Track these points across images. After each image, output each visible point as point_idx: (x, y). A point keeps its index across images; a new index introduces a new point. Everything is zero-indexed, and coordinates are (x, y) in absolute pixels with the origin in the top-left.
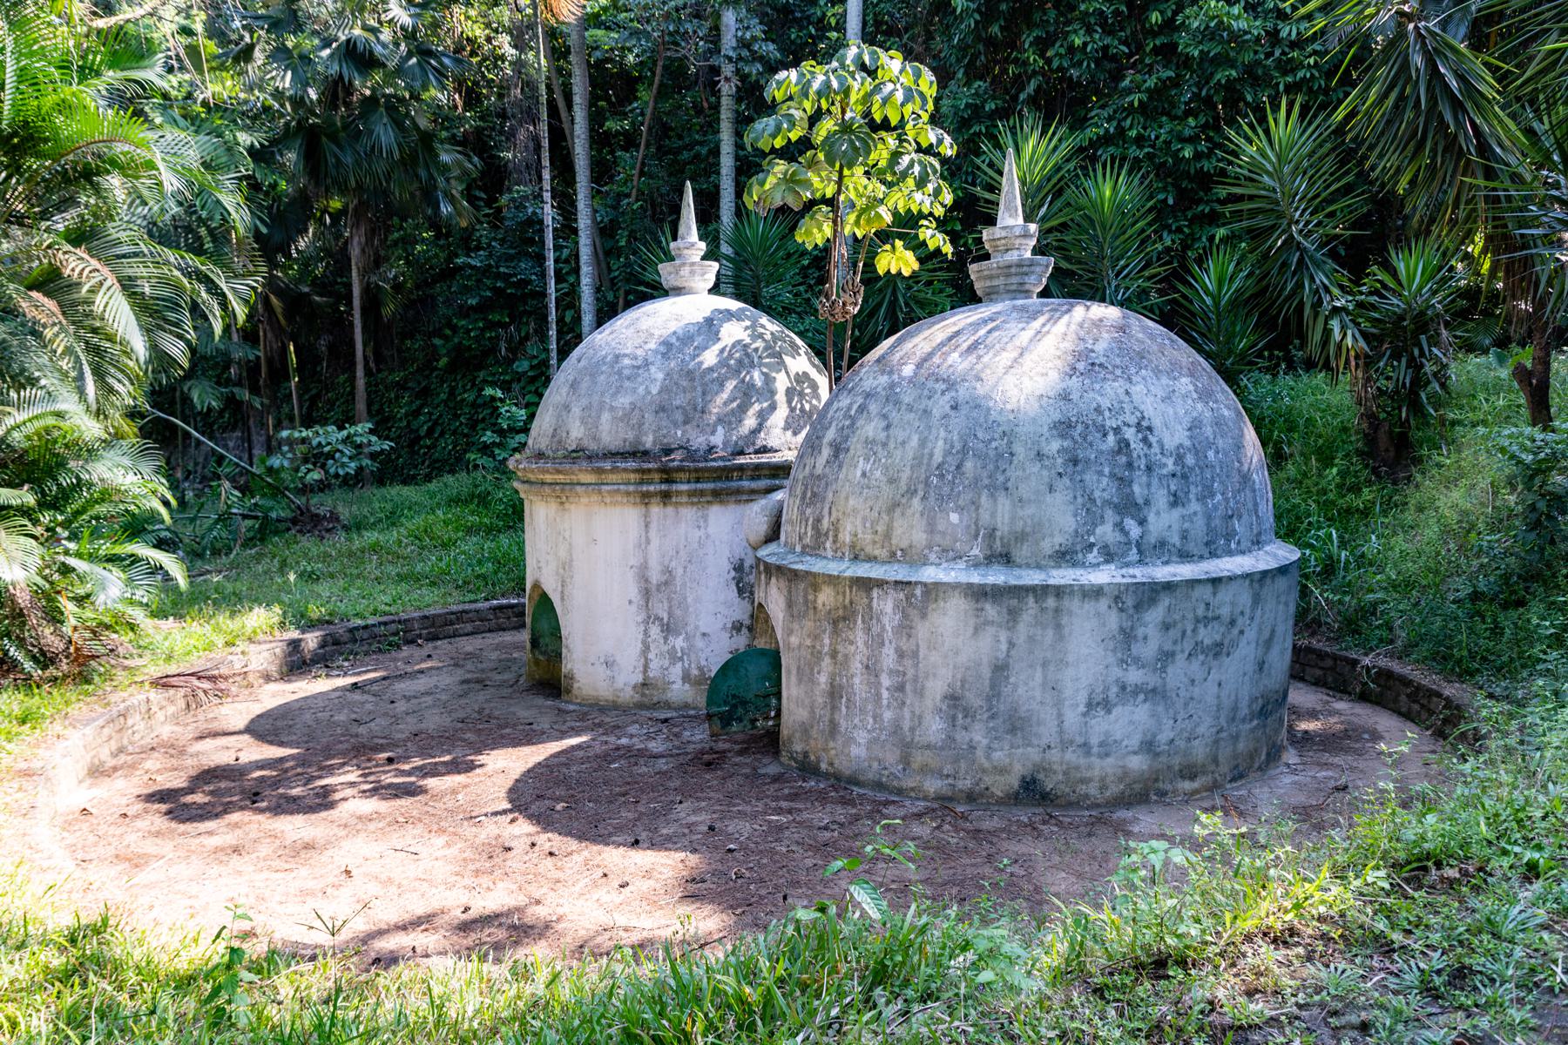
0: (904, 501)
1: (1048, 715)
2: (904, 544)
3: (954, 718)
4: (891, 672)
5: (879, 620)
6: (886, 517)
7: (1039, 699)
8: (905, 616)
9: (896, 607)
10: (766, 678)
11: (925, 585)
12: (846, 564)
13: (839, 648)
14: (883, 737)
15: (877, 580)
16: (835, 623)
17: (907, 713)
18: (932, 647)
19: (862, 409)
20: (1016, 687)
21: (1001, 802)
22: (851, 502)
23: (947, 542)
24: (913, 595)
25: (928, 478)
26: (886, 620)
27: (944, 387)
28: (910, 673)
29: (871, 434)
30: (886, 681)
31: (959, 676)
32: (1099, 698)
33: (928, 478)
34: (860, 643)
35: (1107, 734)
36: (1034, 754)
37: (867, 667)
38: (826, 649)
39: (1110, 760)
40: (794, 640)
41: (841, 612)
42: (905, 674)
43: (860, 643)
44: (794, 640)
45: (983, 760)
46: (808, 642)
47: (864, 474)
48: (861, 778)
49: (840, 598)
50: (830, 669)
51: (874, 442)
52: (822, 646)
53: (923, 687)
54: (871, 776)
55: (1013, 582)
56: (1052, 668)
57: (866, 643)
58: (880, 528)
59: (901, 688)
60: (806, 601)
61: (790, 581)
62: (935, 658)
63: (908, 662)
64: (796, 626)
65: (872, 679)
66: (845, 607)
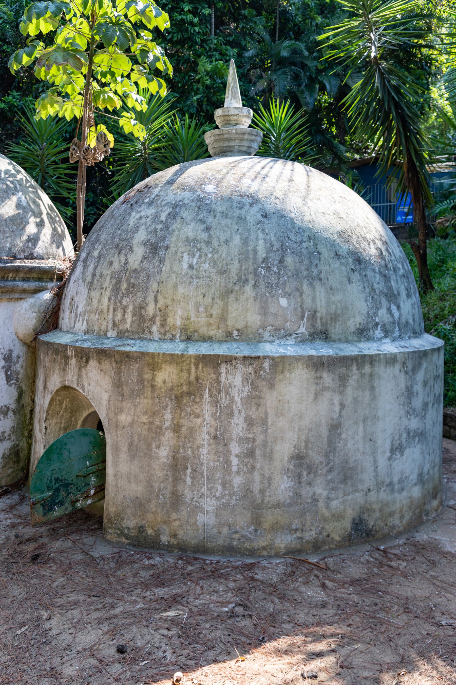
0: (237, 288)
1: (367, 462)
2: (240, 325)
3: (300, 476)
4: (241, 440)
5: (227, 393)
6: (220, 303)
7: (362, 450)
8: (254, 387)
9: (245, 379)
10: (87, 457)
11: (273, 359)
12: (182, 346)
13: (182, 421)
14: (233, 502)
15: (226, 357)
16: (178, 398)
17: (257, 477)
18: (279, 413)
19: (173, 216)
20: (346, 441)
21: (339, 546)
22: (181, 290)
23: (279, 322)
24: (262, 368)
25: (256, 270)
26: (235, 393)
27: (250, 200)
28: (260, 439)
29: (191, 235)
30: (235, 449)
31: (303, 437)
32: (397, 445)
33: (256, 270)
34: (207, 416)
35: (402, 472)
36: (359, 497)
37: (215, 437)
38: (167, 424)
39: (404, 493)
40: (124, 418)
41: (185, 388)
42: (254, 440)
43: (207, 416)
44: (124, 418)
45: (324, 510)
46: (144, 419)
47: (191, 267)
48: (210, 545)
49: (184, 375)
50: (172, 442)
51: (195, 240)
52: (163, 421)
53: (272, 451)
54: (220, 542)
55: (342, 354)
56: (369, 423)
57: (214, 416)
58: (215, 312)
59: (251, 454)
60: (141, 381)
61: (119, 362)
62: (282, 423)
63: (257, 429)
64: (127, 404)
65: (221, 448)
66: (190, 383)
